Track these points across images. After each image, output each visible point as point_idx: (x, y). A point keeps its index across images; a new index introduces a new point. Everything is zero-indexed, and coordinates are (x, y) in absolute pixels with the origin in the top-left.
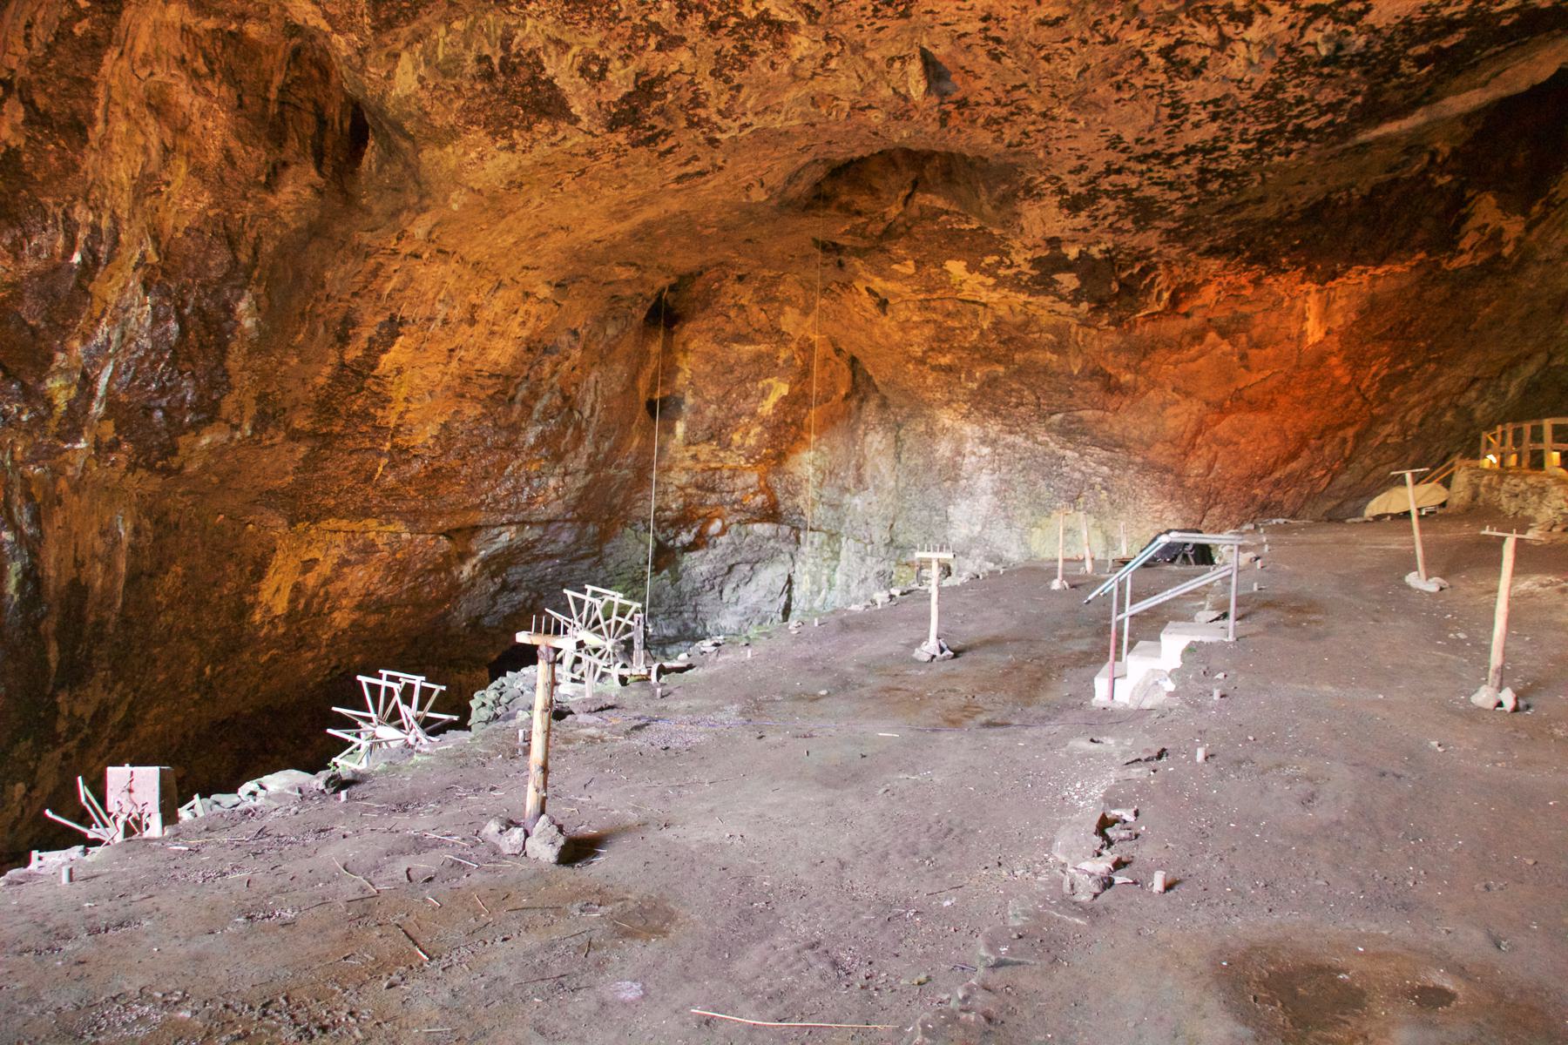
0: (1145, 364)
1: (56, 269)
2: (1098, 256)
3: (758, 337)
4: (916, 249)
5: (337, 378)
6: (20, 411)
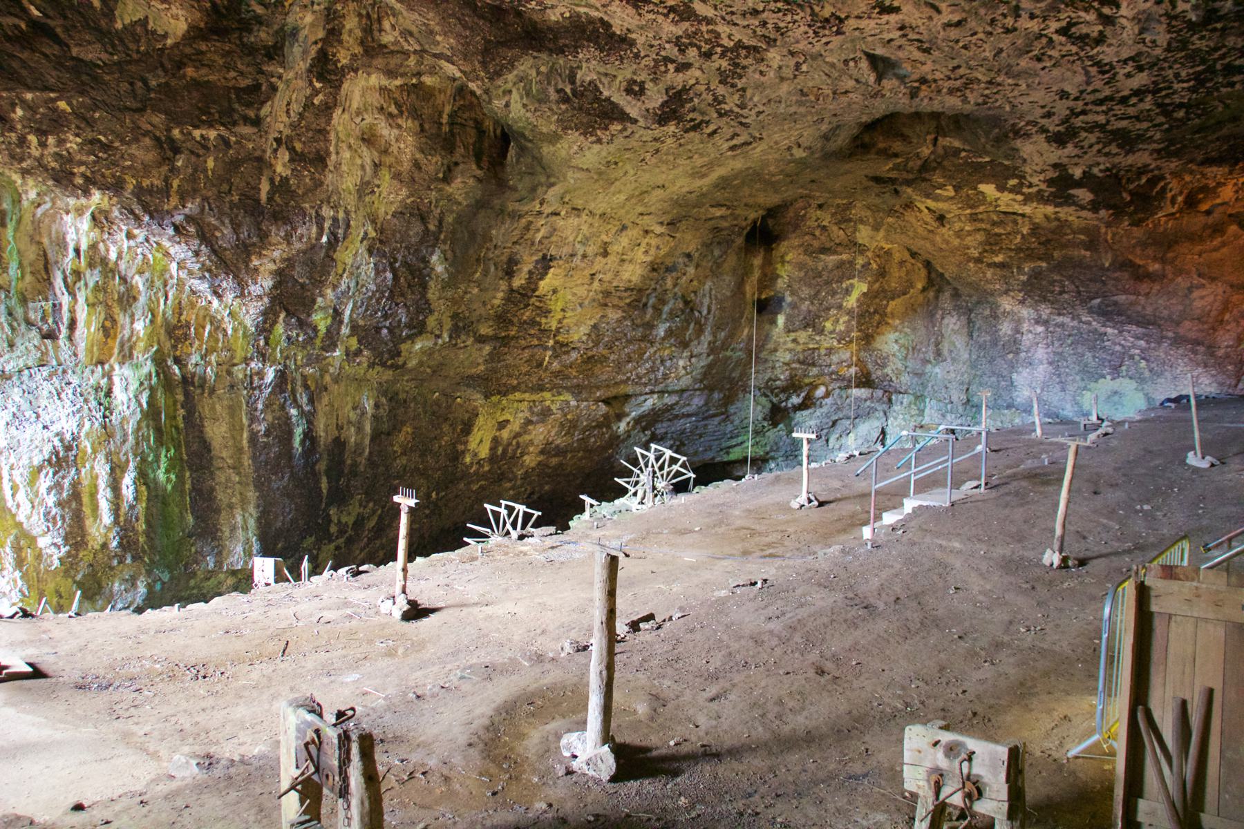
0: (1170, 255)
1: (313, 247)
2: (1100, 175)
3: (840, 249)
4: (951, 177)
5: (508, 300)
6: (298, 335)
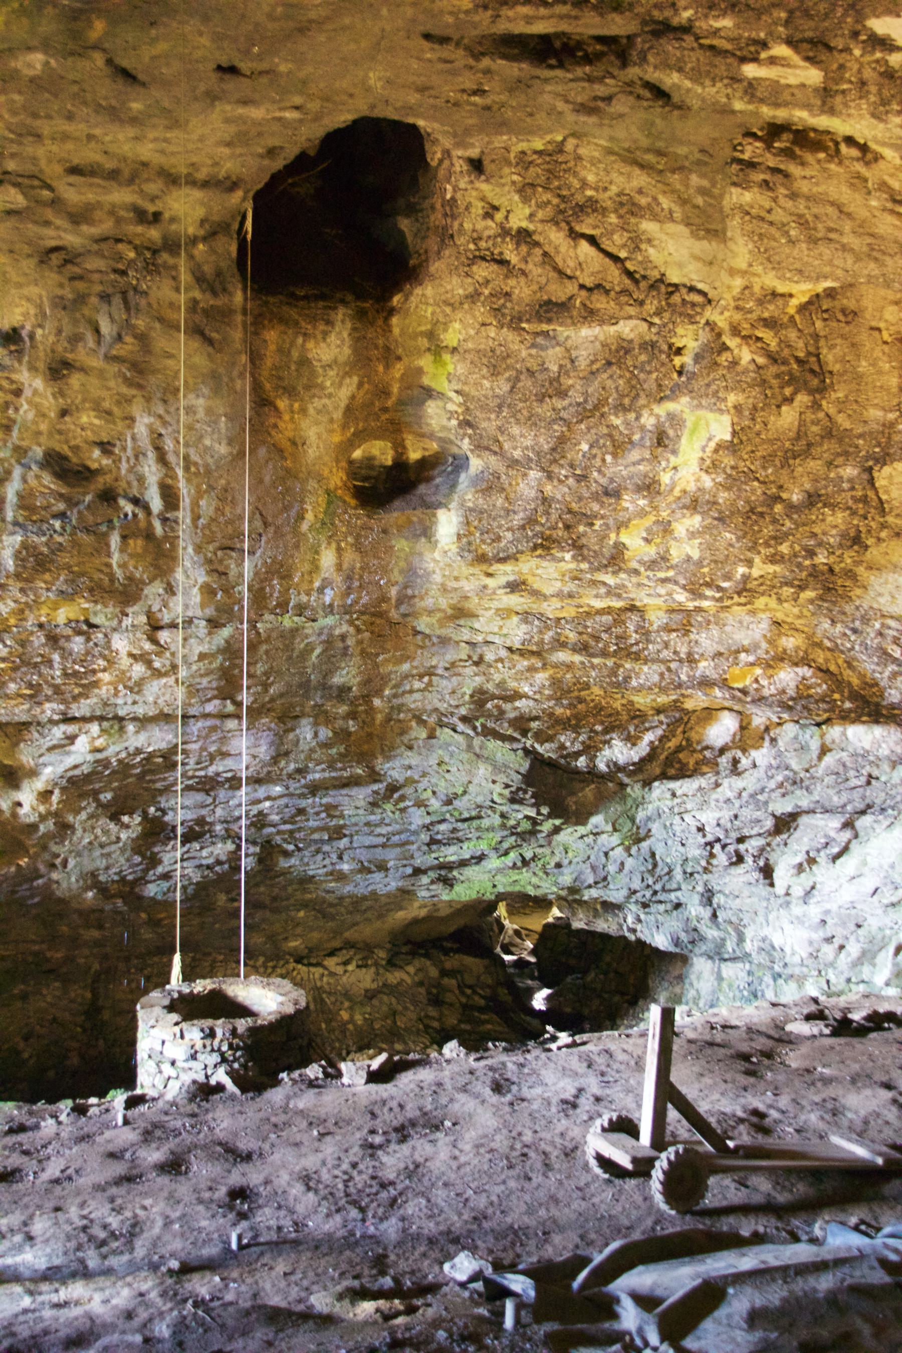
3: (600, 302)
